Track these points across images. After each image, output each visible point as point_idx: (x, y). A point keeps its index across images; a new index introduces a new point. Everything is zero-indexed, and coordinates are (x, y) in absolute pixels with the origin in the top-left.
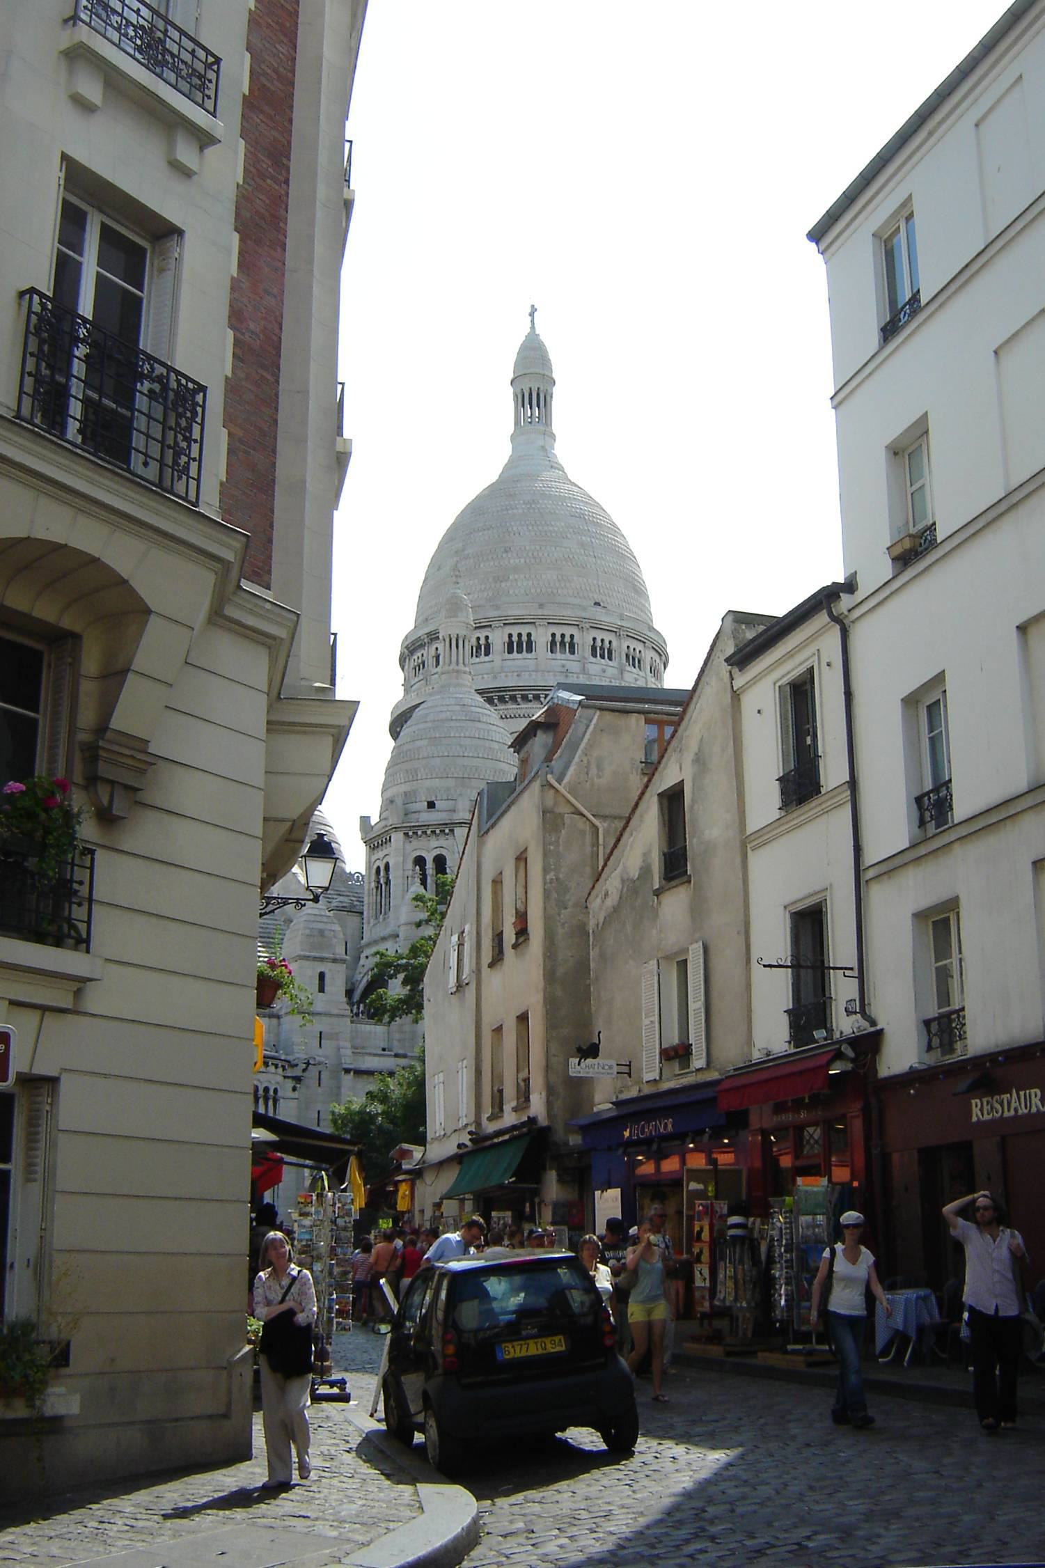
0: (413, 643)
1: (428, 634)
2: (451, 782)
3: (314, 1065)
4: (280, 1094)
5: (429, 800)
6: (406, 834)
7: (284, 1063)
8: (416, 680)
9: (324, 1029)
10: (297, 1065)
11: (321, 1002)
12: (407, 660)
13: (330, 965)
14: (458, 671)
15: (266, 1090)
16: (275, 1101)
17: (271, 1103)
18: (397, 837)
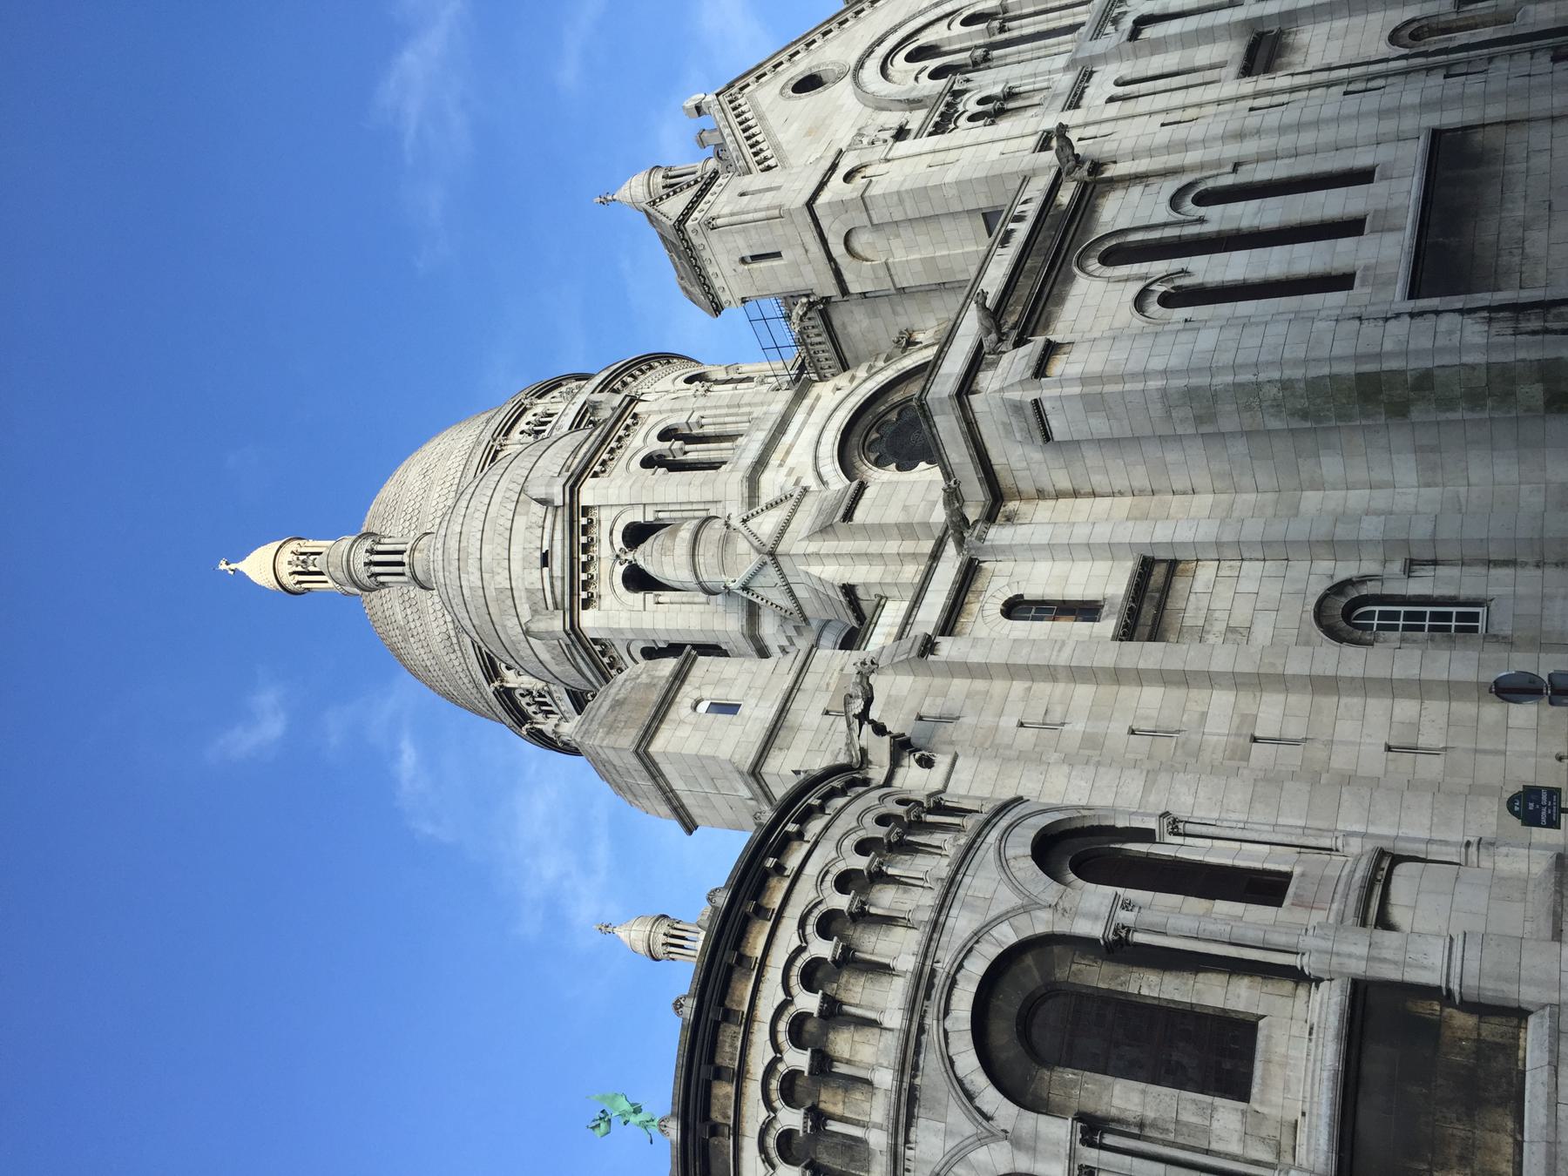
0: (509, 711)
1: (490, 680)
2: (520, 522)
3: (869, 702)
4: (919, 796)
5: (538, 563)
6: (587, 604)
7: (847, 777)
8: (554, 708)
9: (823, 702)
10: (864, 752)
11: (758, 714)
12: (538, 726)
13: (686, 688)
14: (413, 550)
15: (882, 820)
16: (940, 808)
17: (930, 818)
18: (589, 621)
